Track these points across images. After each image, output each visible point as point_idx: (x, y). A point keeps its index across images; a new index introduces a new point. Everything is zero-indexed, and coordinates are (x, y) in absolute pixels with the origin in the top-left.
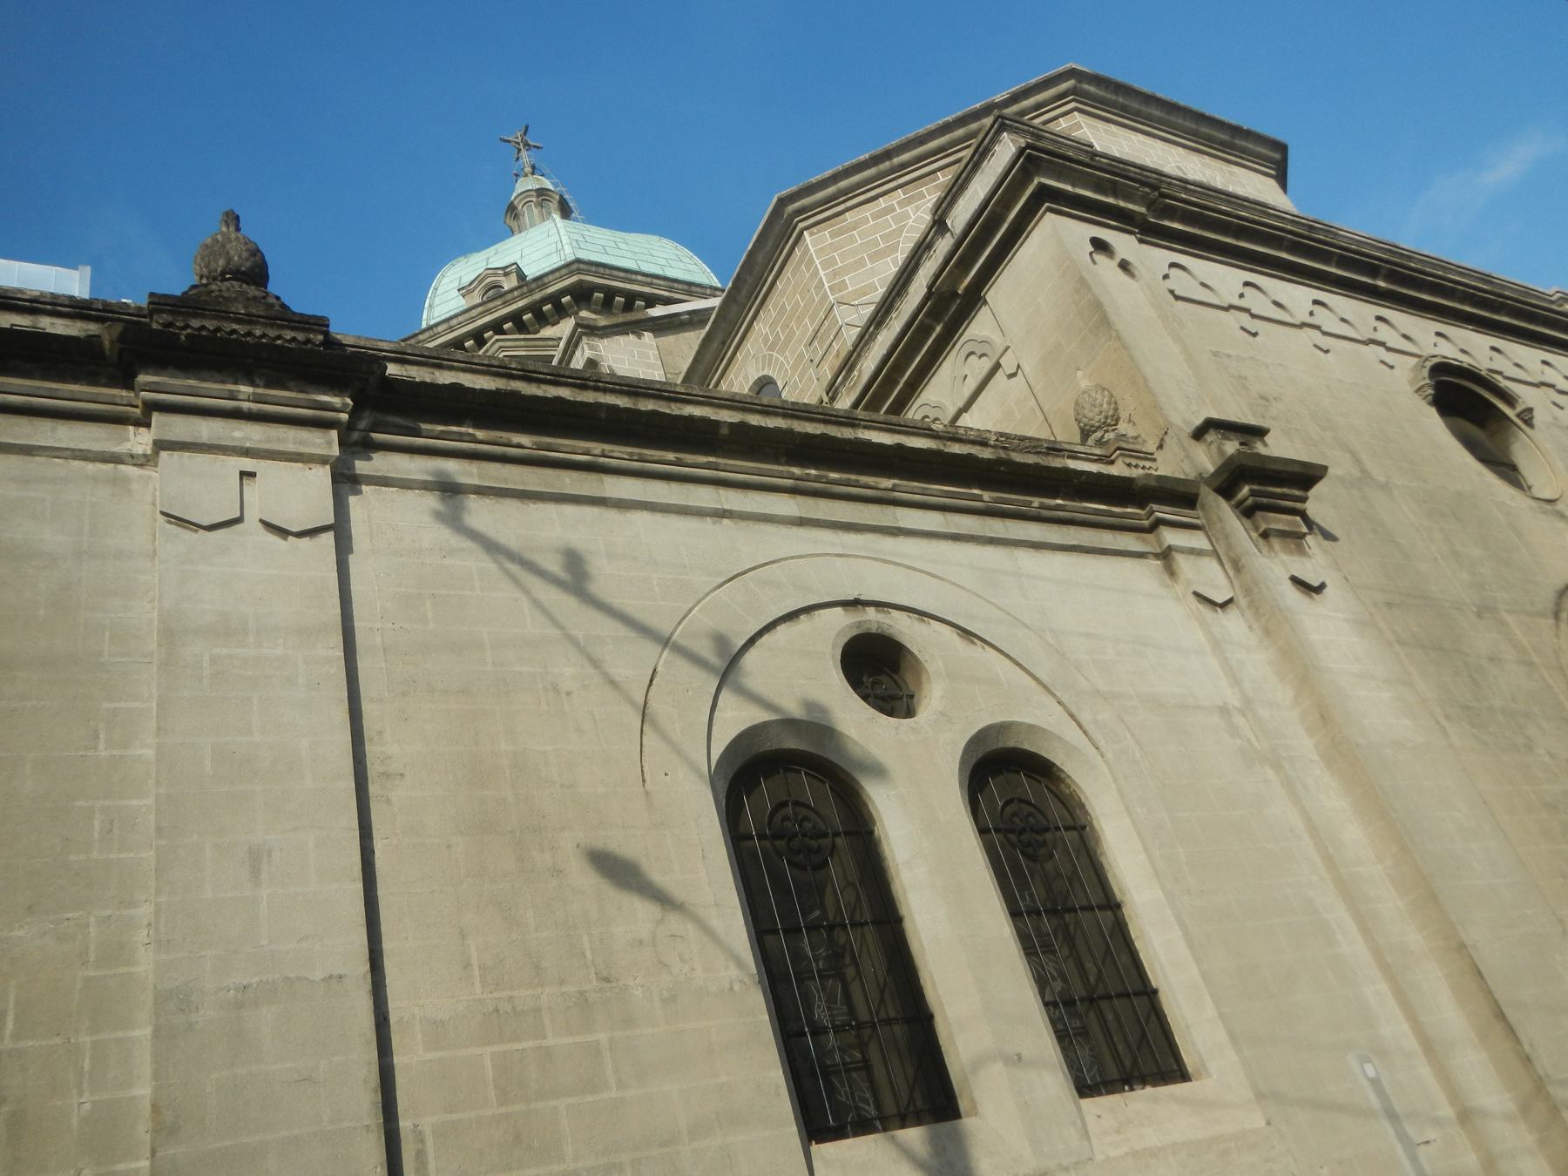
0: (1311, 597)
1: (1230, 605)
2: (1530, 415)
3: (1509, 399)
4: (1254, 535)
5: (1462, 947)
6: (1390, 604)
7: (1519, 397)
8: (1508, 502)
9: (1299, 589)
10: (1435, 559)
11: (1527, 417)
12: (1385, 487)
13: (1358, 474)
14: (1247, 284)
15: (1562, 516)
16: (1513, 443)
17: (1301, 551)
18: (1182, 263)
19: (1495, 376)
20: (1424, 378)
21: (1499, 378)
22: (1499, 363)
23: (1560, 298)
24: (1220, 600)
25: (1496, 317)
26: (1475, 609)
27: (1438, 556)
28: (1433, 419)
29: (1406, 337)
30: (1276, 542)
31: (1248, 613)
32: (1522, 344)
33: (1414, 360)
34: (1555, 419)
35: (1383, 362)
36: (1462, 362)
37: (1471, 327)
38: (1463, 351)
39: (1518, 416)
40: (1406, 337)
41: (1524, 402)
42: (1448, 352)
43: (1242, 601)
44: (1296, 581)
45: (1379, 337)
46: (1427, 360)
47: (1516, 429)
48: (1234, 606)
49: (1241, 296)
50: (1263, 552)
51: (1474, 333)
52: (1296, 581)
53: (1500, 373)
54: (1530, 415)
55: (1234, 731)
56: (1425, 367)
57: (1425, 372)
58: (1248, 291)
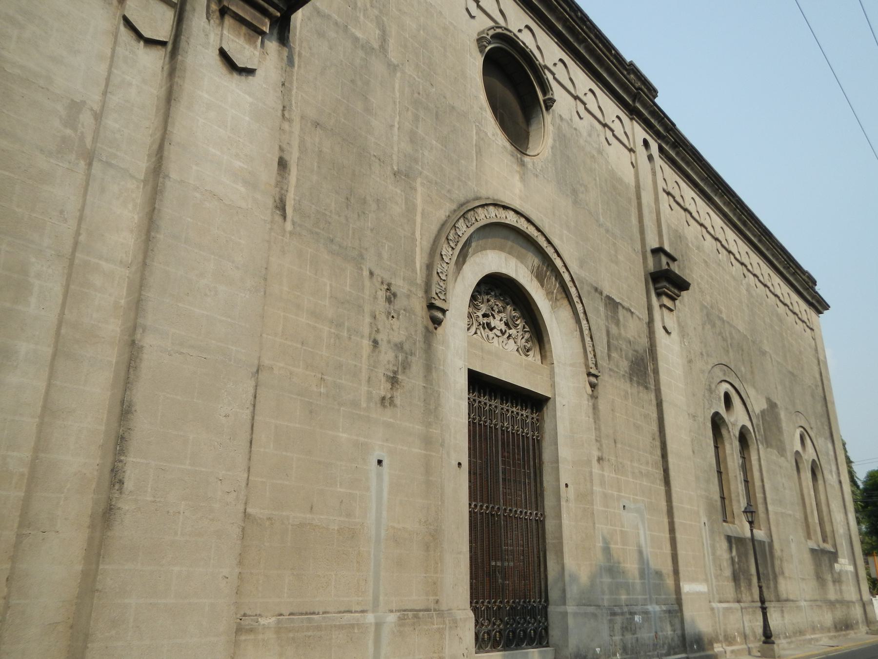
0: (231, 73)
1: (160, 47)
2: (551, 104)
3: (545, 89)
4: (214, 7)
5: (133, 343)
6: (318, 124)
7: (552, 90)
8: (490, 134)
9: (222, 61)
10: (392, 126)
11: (549, 104)
12: (393, 68)
13: (376, 45)
14: (561, 60)
15: (522, 164)
16: (534, 117)
17: (250, 41)
18: (535, 33)
19: (546, 72)
20: (488, 35)
21: (550, 76)
22: (560, 71)
23: (632, 69)
24: (147, 34)
25: (576, 45)
26: (395, 168)
27: (397, 126)
28: (476, 62)
29: (501, 12)
30: (228, 21)
31: (168, 55)
32: (583, 71)
33: (492, 24)
34: (571, 120)
35: (467, 10)
36: (527, 47)
37: (556, 40)
38: (538, 48)
39: (544, 101)
40: (501, 12)
41: (552, 95)
42: (526, 38)
43: (170, 46)
44: (223, 54)
45: (584, 99)
46: (501, 27)
47: (539, 109)
48: (164, 50)
49: (520, 31)
50: (212, 21)
51: (556, 45)
52: (223, 54)
53: (553, 74)
54: (551, 104)
55: (71, 121)
56: (495, 30)
57: (491, 32)
58: (560, 65)
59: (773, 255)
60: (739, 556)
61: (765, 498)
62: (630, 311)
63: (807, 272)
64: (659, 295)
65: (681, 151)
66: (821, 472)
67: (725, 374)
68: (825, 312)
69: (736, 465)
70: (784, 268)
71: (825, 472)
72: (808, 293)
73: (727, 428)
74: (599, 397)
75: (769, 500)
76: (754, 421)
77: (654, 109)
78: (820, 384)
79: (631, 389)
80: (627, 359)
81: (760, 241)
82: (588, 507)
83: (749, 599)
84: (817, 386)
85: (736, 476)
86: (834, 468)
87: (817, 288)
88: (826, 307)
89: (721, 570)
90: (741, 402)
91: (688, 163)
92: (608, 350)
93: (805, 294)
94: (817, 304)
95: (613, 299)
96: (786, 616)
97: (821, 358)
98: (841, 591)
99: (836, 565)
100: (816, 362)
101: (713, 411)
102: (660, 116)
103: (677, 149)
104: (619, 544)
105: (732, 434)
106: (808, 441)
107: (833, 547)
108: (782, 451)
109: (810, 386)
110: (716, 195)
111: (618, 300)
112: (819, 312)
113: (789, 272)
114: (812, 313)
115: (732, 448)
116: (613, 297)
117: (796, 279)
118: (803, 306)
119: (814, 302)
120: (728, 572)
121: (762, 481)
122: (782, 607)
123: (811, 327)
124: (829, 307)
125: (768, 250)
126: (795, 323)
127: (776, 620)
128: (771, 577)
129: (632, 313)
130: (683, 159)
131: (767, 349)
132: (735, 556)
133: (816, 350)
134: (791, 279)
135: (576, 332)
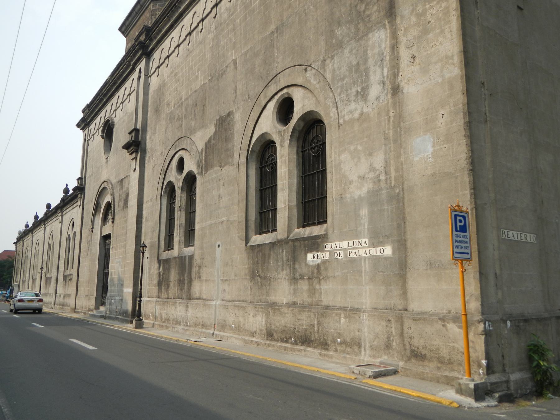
60: (164, 270)
65: (153, 36)
77: (133, 55)
83: (166, 296)
89: (152, 280)
91: (160, 31)
96: (190, 310)
98: (312, 292)
99: (310, 256)
102: (135, 52)
103: (153, 38)
110: (180, 8)
120: (156, 281)
122: (188, 303)
127: (180, 312)
128: (186, 281)
130: (158, 34)
132: (161, 272)
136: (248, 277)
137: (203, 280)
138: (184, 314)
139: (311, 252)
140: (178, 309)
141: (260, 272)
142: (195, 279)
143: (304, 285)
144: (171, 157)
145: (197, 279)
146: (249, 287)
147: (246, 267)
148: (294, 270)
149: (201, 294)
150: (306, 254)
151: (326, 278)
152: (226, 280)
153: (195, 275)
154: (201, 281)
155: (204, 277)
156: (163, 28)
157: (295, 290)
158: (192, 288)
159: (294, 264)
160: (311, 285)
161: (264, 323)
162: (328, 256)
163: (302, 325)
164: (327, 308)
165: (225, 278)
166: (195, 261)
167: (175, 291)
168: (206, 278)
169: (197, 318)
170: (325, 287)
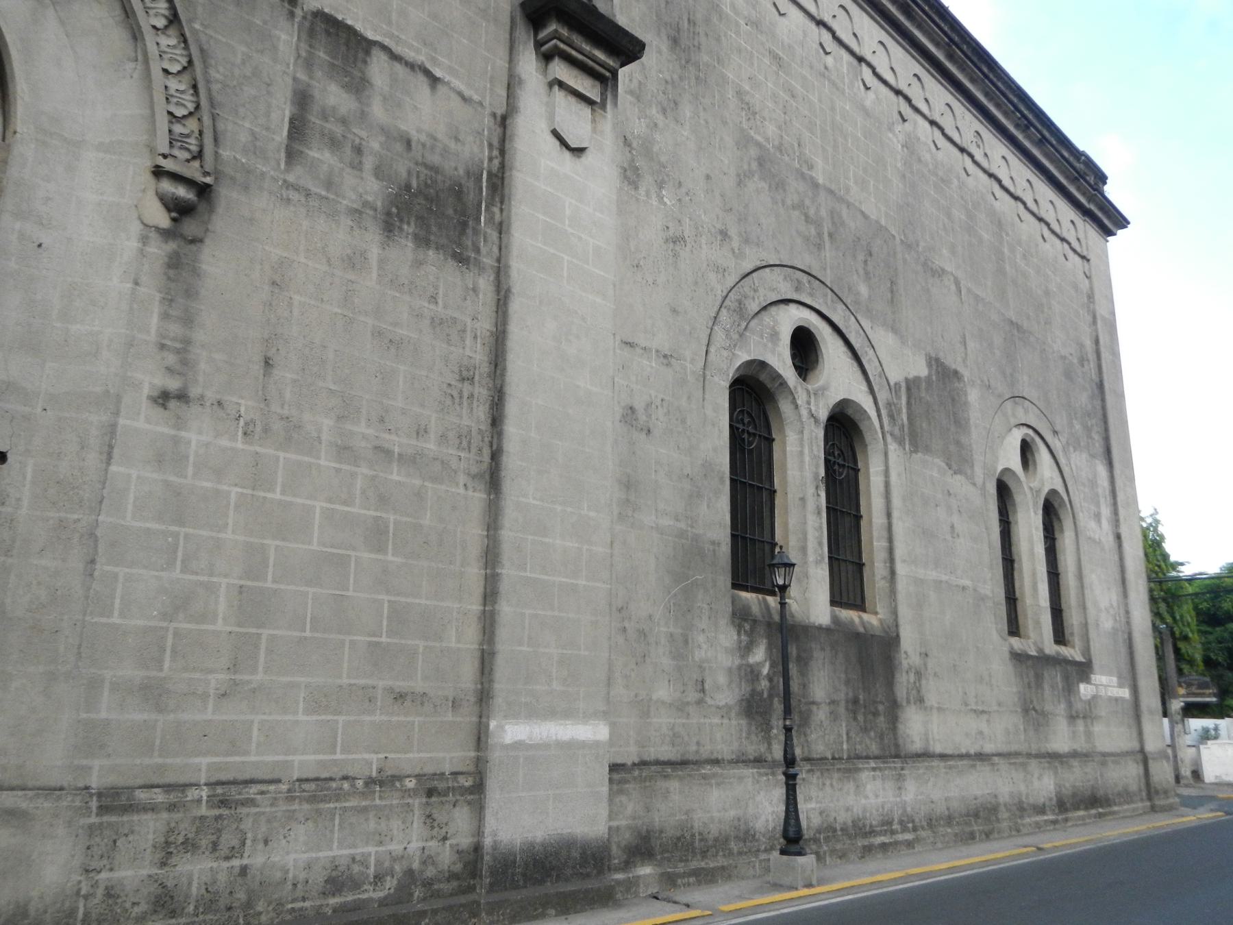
59: (986, 95)
61: (891, 551)
62: (427, 73)
63: (1083, 154)
64: (547, 58)
66: (1071, 515)
67: (797, 289)
68: (1120, 232)
69: (809, 475)
70: (1017, 126)
71: (1082, 517)
72: (1078, 189)
73: (790, 398)
74: (207, 241)
75: (899, 552)
76: (883, 396)
78: (1092, 356)
79: (383, 246)
80: (378, 173)
81: (951, 57)
82: (76, 516)
84: (1083, 360)
85: (803, 499)
86: (1106, 511)
87: (1106, 188)
88: (1122, 222)
90: (850, 354)
92: (291, 136)
93: (1072, 189)
94: (1100, 214)
95: (351, 30)
97: (1101, 311)
98: (1089, 735)
99: (1083, 687)
100: (1089, 318)
101: (744, 357)
104: (116, 613)
105: (804, 412)
106: (1043, 456)
107: (1083, 655)
108: (959, 461)
109: (1064, 358)
111: (370, 35)
112: (1110, 233)
113: (1028, 137)
114: (1089, 232)
115: (802, 440)
116: (349, 22)
117: (1047, 155)
118: (1066, 212)
119: (1092, 207)
121: (889, 515)
123: (1085, 253)
124: (1129, 223)
125: (972, 80)
126: (1041, 240)
127: (877, 796)
129: (434, 81)
131: (944, 260)
132: (760, 664)
133: (1091, 297)
134: (1036, 152)
135: (132, 65)
136: (1019, 710)
137: (931, 708)
138: (891, 799)
139: (1082, 682)
140: (869, 787)
141: (1035, 702)
142: (908, 702)
143: (1080, 726)
144: (844, 331)
145: (915, 704)
146: (1022, 727)
147: (1015, 690)
148: (1070, 705)
149: (927, 740)
150: (1078, 684)
151: (1097, 718)
152: (983, 712)
153: (907, 693)
154: (926, 709)
155: (932, 699)
156: (998, 106)
157: (1074, 732)
158: (900, 726)
159: (1069, 695)
160: (1086, 726)
161: (1052, 787)
162: (1095, 690)
163: (1089, 781)
164: (1104, 755)
165: (980, 708)
166: (903, 656)
167: (840, 735)
168: (939, 703)
169: (932, 802)
170: (1098, 728)
